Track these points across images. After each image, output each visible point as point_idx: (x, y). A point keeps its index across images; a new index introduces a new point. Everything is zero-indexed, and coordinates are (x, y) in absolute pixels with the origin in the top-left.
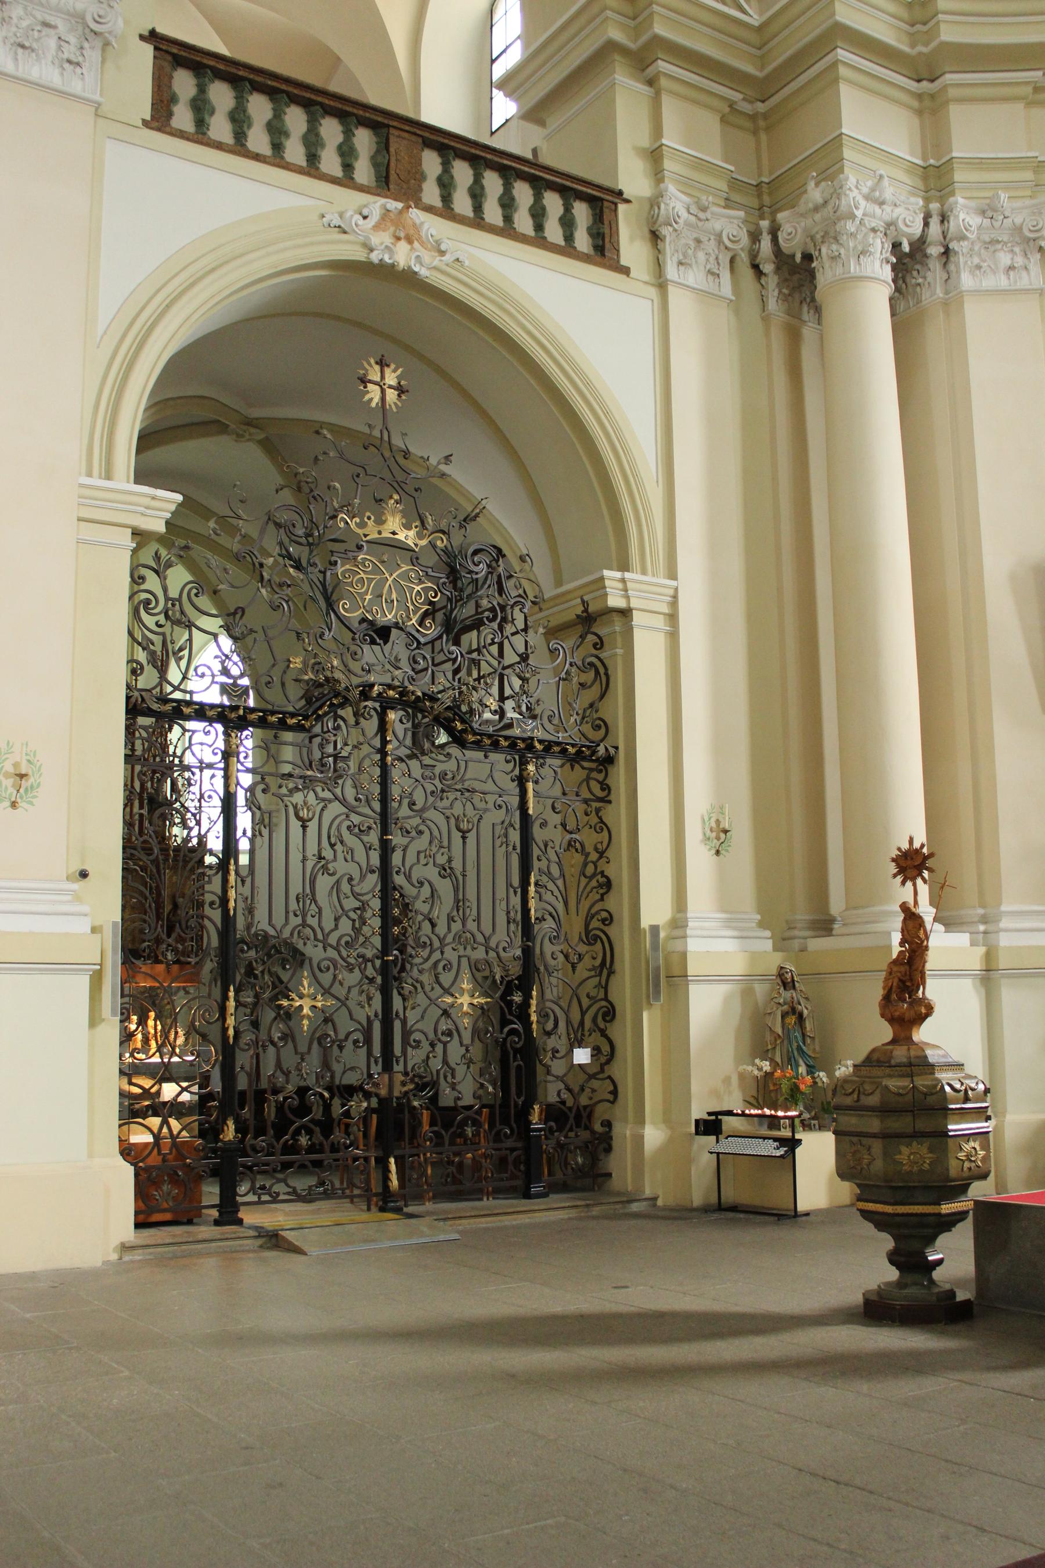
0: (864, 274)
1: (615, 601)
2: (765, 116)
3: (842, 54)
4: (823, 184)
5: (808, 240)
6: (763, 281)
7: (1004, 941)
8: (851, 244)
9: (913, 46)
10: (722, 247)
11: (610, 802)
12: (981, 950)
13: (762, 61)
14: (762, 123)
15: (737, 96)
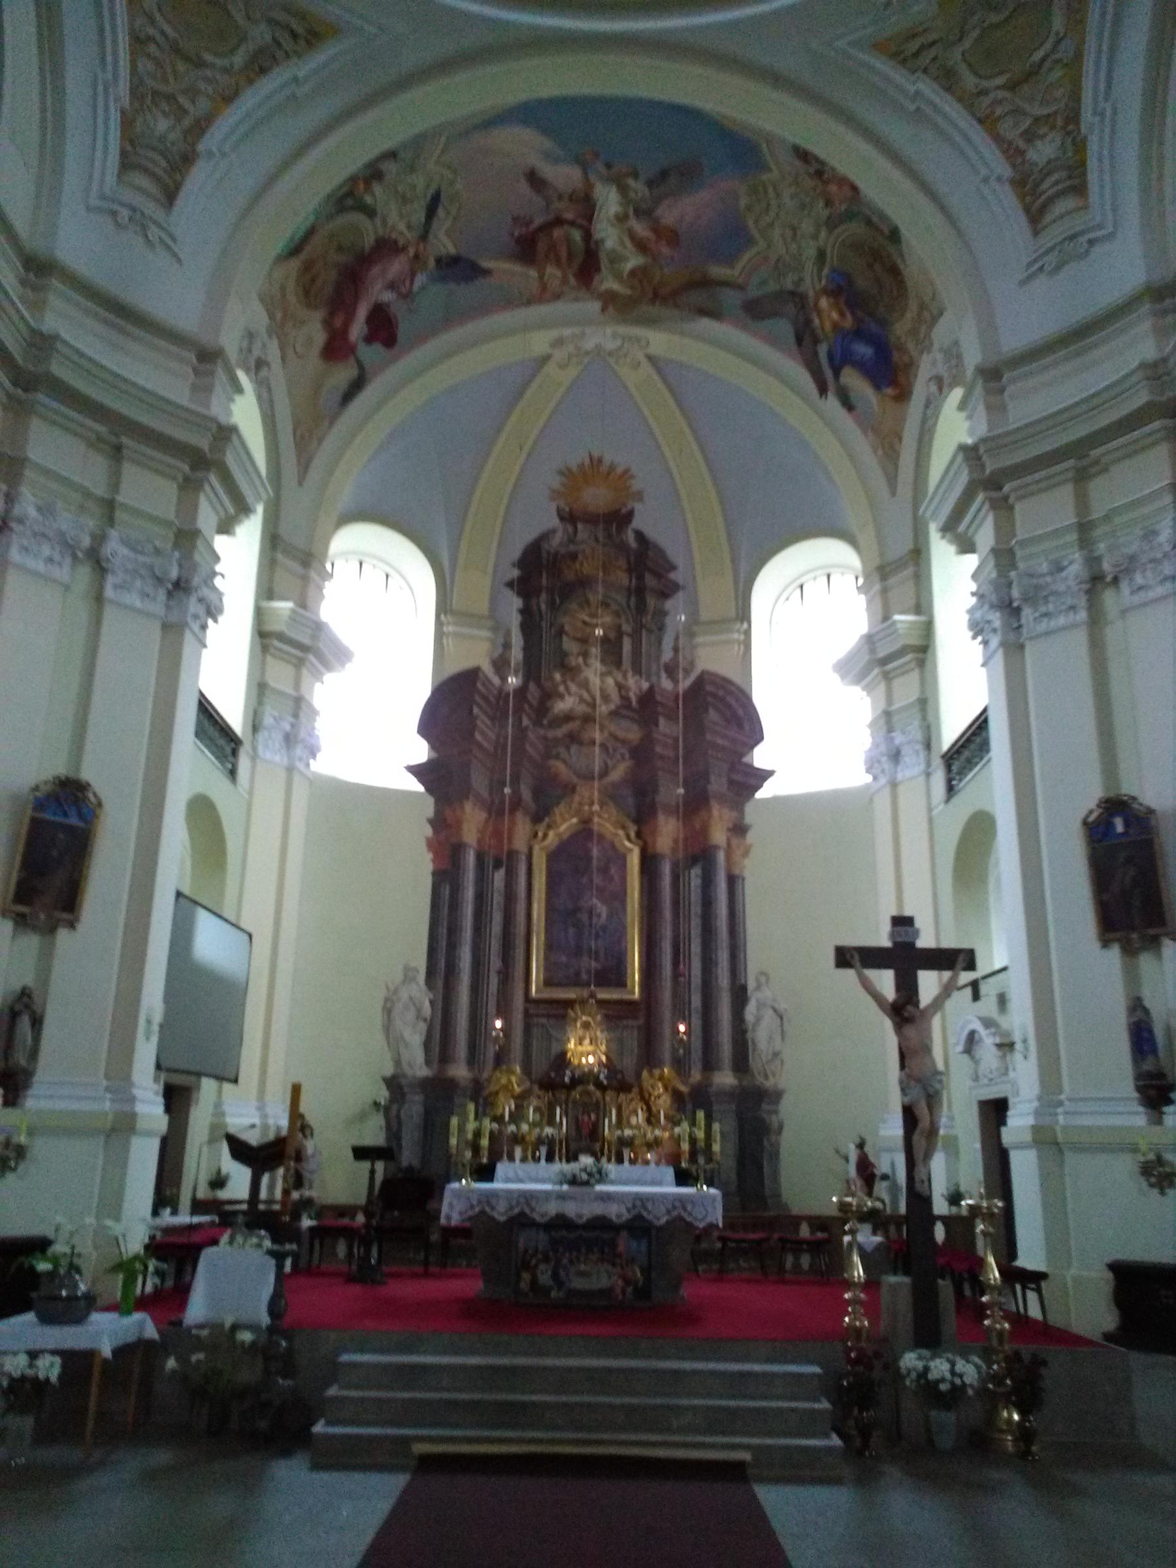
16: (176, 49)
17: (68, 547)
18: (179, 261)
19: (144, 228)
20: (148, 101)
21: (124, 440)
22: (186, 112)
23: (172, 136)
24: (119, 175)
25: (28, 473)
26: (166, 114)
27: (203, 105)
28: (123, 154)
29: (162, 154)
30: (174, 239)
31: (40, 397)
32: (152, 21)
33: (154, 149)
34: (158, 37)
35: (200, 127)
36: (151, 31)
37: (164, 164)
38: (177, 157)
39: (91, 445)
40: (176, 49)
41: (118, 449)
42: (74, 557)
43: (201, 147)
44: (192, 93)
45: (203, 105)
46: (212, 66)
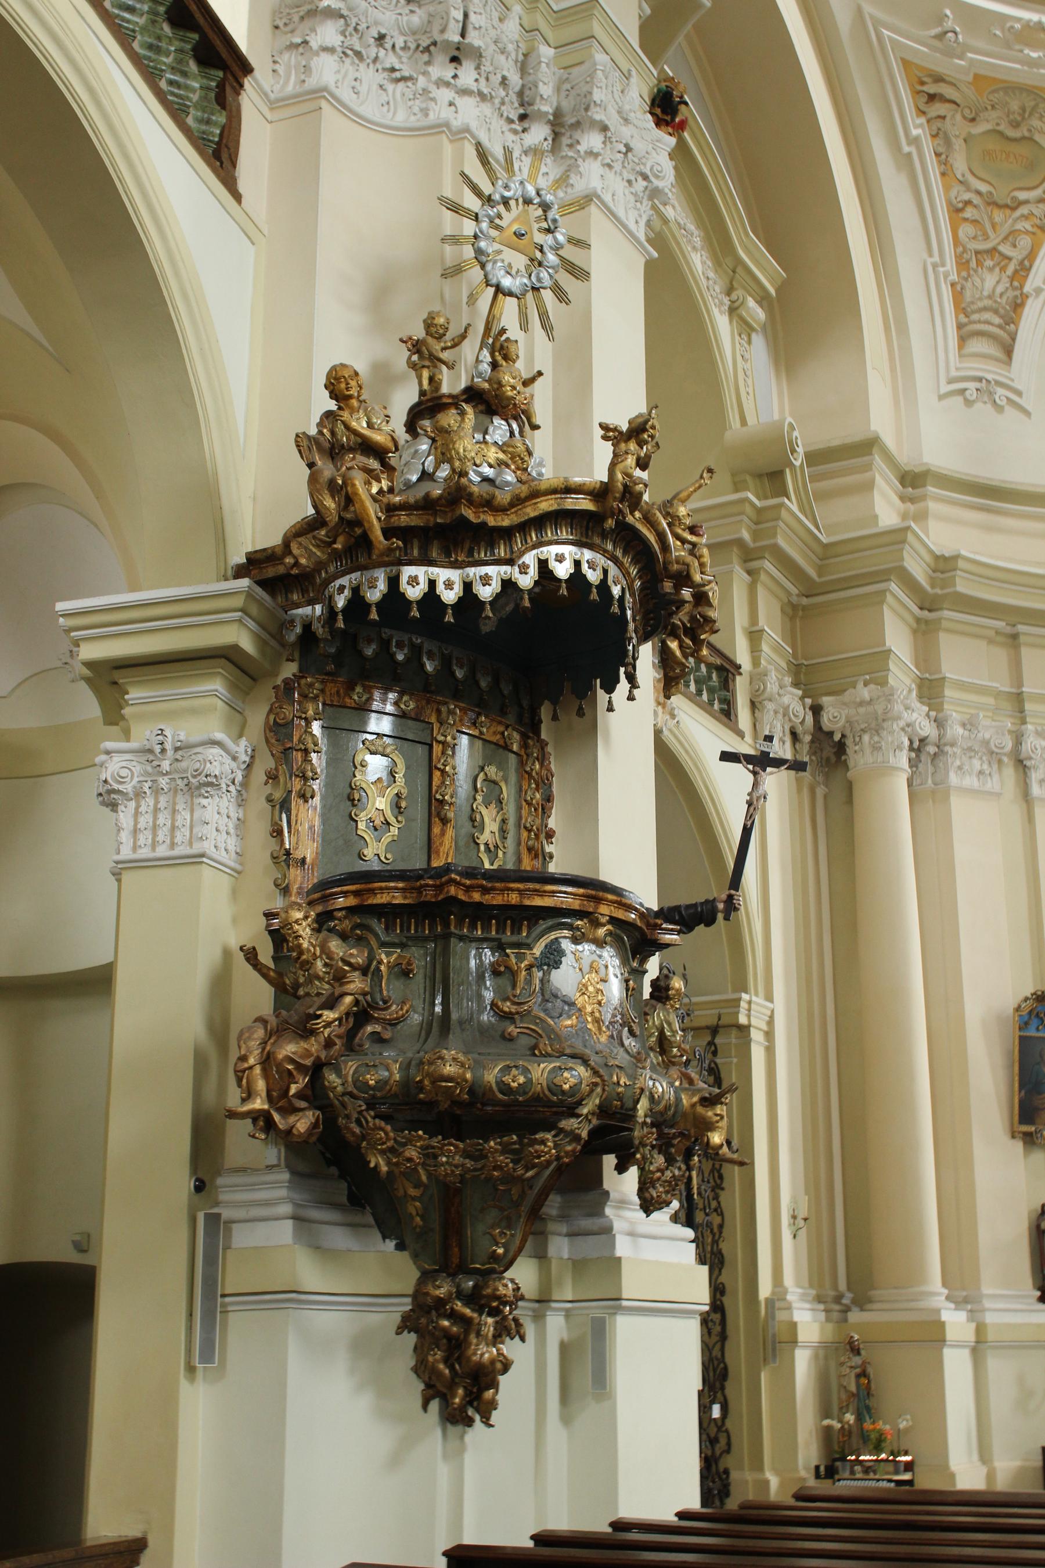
0: (898, 765)
1: (743, 1020)
2: (804, 608)
3: (893, 587)
4: (872, 686)
5: (847, 725)
6: (797, 746)
7: (990, 1318)
8: (890, 739)
9: (933, 587)
10: (787, 718)
11: (723, 1189)
12: (973, 1325)
13: (821, 570)
14: (800, 613)
15: (794, 591)
16: (992, 203)
17: (993, 756)
18: (1027, 413)
19: (991, 394)
20: (973, 264)
21: (1021, 628)
22: (1010, 259)
23: (1000, 289)
24: (961, 346)
25: (948, 692)
26: (991, 269)
27: (1025, 242)
28: (960, 326)
29: (996, 312)
30: (1019, 394)
31: (946, 614)
32: (968, 189)
33: (985, 309)
34: (976, 200)
35: (1024, 269)
36: (967, 196)
37: (997, 320)
38: (1008, 307)
39: (991, 641)
40: (992, 203)
41: (1015, 637)
42: (1000, 762)
43: (1027, 288)
44: (1011, 237)
45: (1025, 242)
46: (1026, 202)
